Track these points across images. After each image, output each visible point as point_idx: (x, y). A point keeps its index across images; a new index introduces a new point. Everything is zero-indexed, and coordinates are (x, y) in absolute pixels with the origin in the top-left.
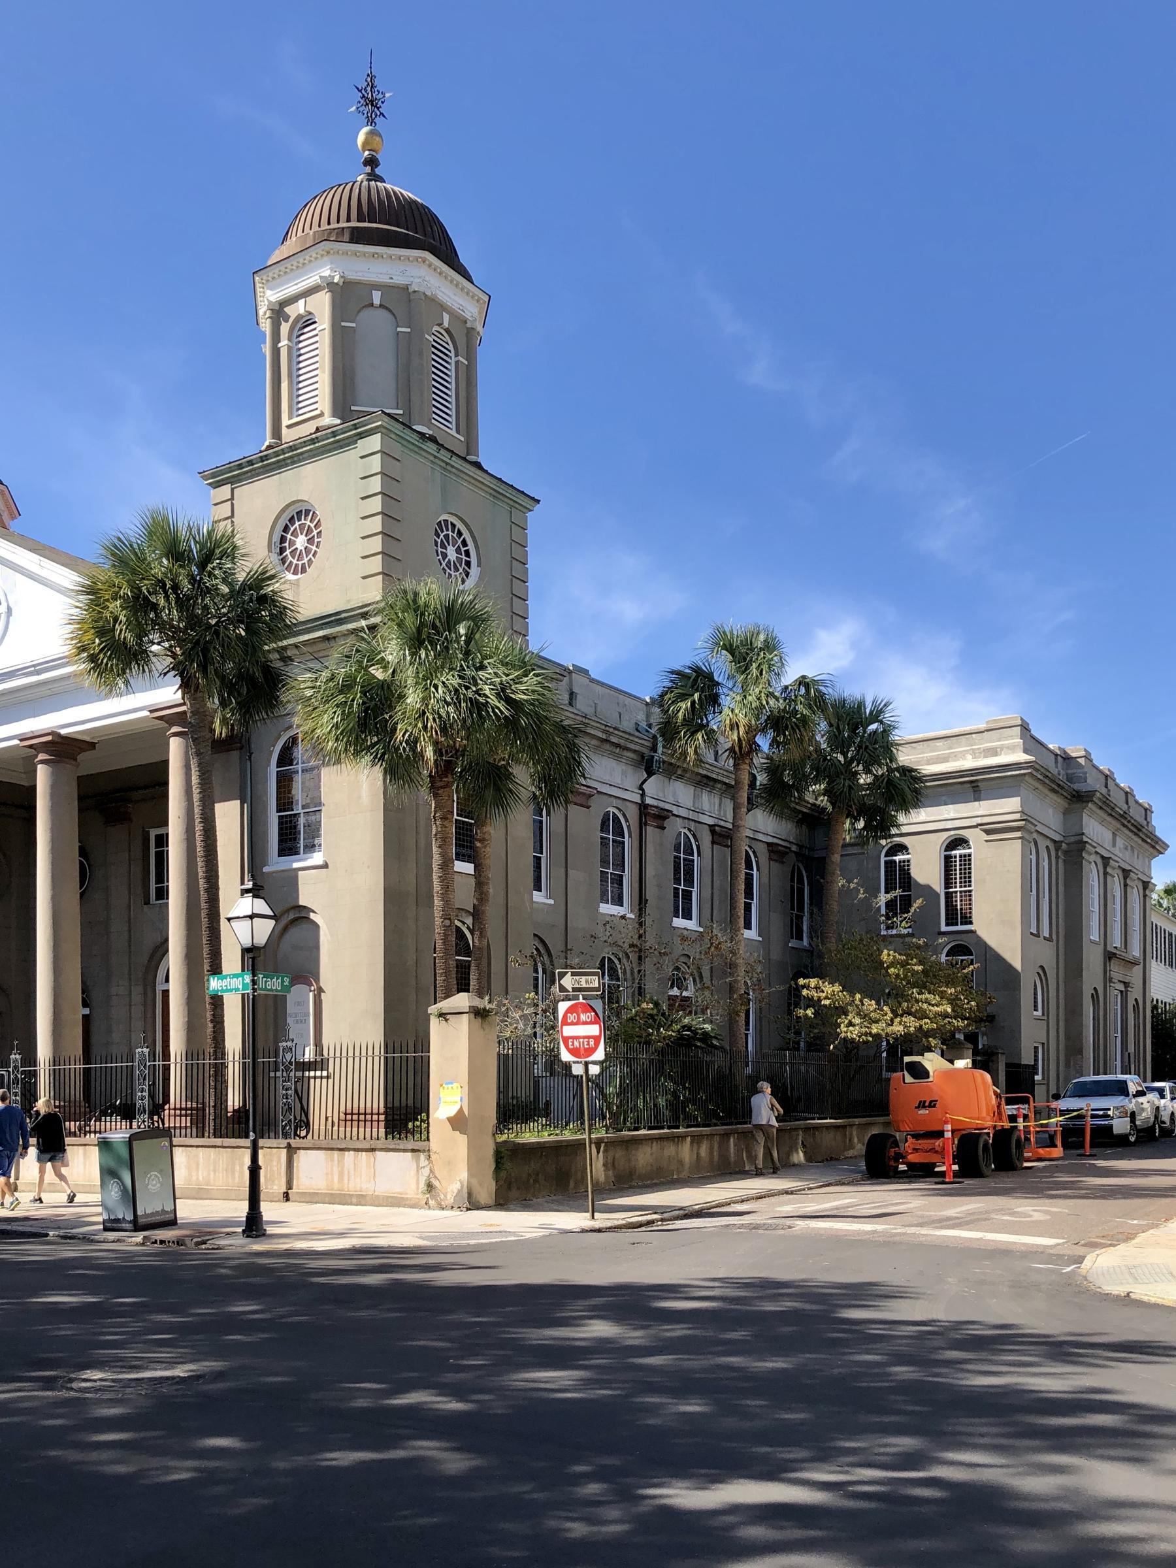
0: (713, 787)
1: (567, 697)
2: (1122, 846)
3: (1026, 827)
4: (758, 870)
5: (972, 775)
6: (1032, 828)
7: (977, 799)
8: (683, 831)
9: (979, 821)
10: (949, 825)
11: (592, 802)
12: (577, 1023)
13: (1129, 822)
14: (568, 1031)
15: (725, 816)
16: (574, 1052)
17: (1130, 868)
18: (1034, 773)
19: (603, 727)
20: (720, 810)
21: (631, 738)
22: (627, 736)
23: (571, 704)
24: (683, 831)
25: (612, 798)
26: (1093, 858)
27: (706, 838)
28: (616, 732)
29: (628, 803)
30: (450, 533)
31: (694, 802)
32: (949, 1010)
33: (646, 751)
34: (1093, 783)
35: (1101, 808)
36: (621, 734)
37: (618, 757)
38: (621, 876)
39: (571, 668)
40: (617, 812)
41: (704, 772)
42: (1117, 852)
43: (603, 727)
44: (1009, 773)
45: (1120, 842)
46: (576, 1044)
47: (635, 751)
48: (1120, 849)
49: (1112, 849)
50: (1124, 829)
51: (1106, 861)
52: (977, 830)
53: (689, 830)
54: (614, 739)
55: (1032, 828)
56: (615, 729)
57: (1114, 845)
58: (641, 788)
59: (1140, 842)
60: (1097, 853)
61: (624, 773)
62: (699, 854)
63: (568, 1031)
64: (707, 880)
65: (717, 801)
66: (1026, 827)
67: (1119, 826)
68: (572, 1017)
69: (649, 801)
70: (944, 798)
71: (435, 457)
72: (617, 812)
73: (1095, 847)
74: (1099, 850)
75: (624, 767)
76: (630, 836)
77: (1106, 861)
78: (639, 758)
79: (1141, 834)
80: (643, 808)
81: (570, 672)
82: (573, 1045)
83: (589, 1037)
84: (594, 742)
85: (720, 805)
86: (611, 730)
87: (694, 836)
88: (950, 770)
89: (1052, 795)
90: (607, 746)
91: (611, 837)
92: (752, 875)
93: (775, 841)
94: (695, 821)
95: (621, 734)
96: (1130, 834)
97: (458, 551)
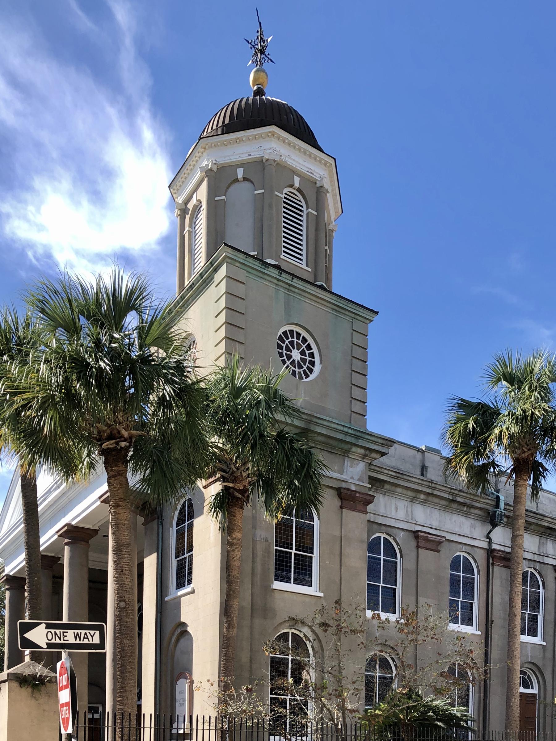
19: (449, 490)
22: (472, 497)
28: (462, 494)
31: (539, 548)
33: (490, 508)
40: (466, 555)
43: (449, 490)
47: (481, 509)
54: (459, 499)
56: (460, 491)
61: (472, 526)
72: (466, 555)
75: (472, 521)
78: (486, 514)
84: (444, 502)
86: (456, 492)
90: (455, 506)
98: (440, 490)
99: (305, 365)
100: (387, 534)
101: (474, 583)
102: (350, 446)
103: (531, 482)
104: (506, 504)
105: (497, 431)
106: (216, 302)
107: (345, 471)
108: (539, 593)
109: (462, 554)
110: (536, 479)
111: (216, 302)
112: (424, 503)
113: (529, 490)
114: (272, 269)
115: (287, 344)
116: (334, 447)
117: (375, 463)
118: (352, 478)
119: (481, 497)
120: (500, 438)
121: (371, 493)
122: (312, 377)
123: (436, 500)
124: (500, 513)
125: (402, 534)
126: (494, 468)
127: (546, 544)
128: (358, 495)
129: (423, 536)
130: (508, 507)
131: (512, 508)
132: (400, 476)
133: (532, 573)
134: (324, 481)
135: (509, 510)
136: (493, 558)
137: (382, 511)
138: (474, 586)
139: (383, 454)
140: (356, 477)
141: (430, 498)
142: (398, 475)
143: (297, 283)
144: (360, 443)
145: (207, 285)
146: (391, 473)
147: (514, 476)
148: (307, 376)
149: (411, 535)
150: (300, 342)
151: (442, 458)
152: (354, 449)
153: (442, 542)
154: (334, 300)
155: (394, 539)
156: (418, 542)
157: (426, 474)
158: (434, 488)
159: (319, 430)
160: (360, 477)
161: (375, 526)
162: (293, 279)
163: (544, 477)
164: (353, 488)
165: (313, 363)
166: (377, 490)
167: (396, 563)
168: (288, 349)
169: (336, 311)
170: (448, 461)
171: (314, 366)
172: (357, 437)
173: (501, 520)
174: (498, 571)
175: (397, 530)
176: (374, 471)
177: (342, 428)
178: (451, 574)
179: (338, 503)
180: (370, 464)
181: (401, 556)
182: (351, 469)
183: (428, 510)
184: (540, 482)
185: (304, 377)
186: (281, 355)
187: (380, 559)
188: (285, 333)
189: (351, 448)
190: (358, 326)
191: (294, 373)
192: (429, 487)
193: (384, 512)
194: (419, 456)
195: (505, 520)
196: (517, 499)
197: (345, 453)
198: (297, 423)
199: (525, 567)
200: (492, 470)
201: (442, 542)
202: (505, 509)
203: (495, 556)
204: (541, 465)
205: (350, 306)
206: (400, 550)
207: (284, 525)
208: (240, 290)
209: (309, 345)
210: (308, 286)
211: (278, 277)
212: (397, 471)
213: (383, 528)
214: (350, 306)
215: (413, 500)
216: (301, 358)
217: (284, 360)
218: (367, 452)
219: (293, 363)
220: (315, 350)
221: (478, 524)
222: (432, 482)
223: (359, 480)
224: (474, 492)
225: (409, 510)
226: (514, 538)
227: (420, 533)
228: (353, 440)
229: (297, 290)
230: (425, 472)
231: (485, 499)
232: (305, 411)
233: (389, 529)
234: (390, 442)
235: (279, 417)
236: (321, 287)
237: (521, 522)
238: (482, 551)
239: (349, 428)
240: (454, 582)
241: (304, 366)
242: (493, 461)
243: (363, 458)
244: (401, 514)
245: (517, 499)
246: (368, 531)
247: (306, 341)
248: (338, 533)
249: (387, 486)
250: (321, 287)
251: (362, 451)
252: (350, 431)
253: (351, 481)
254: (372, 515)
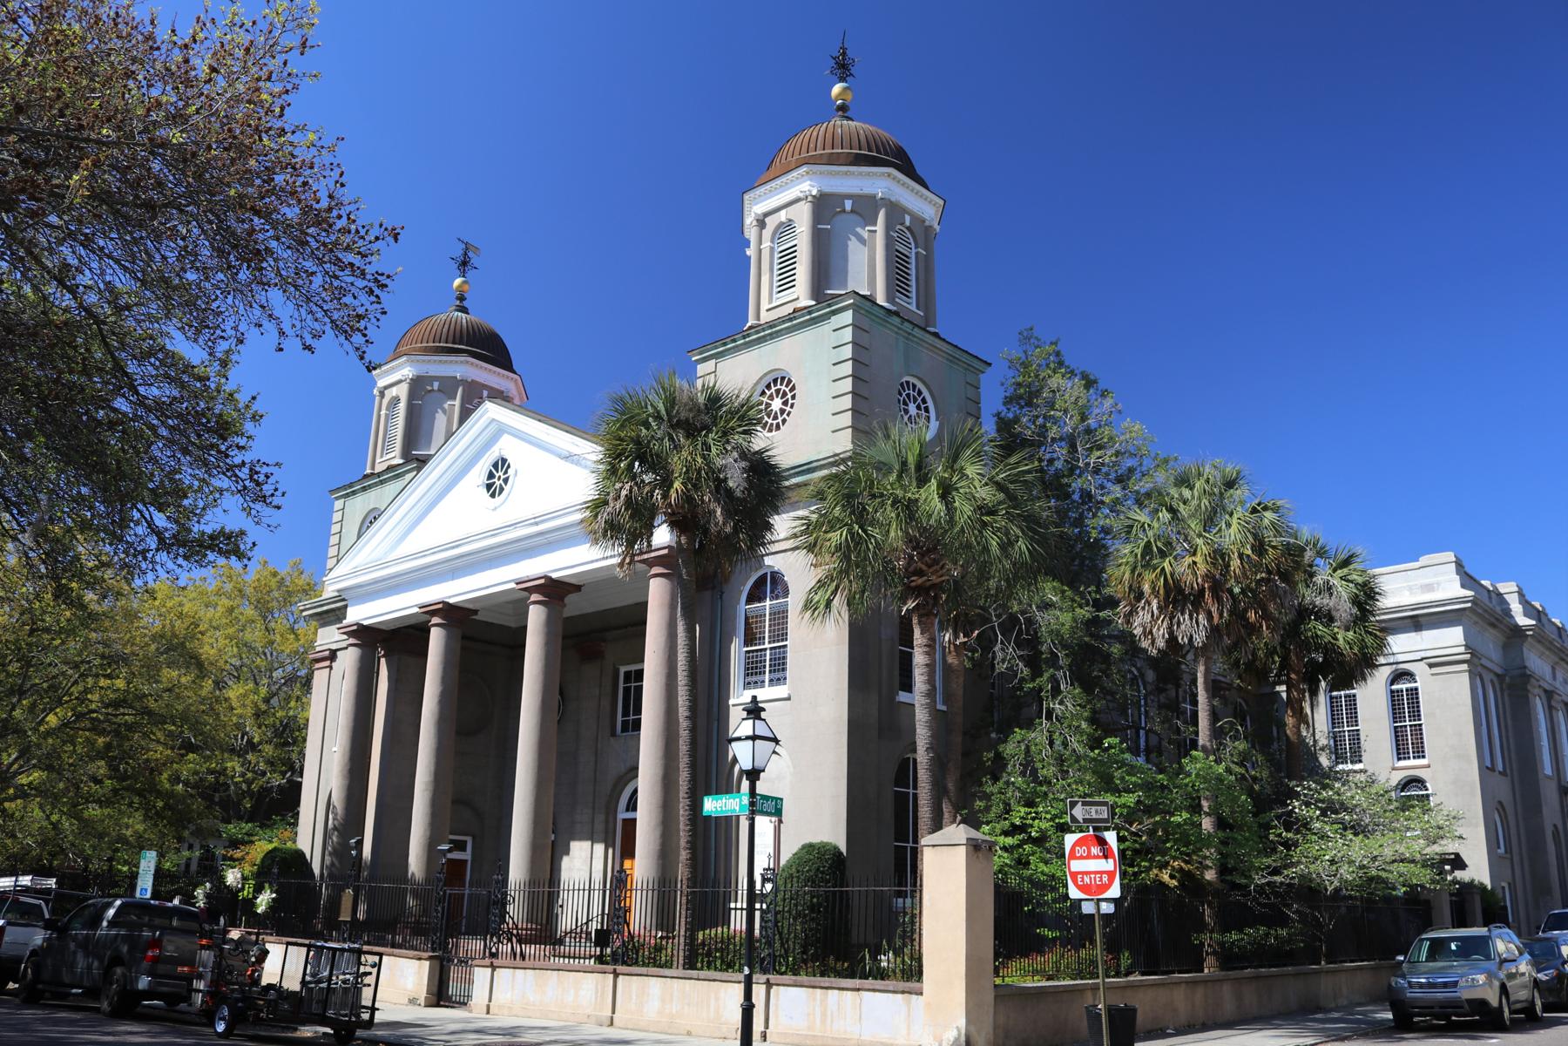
12: (1089, 857)
14: (1076, 866)
16: (1082, 888)
26: (1537, 691)
30: (911, 392)
42: (1558, 684)
46: (1087, 880)
50: (1562, 663)
55: (1475, 660)
57: (1554, 678)
60: (1540, 686)
63: (1076, 866)
68: (1080, 851)
71: (899, 328)
73: (1538, 681)
74: (1542, 683)
77: (1549, 694)
82: (1083, 881)
83: (1102, 873)
89: (1492, 630)
97: (918, 408)
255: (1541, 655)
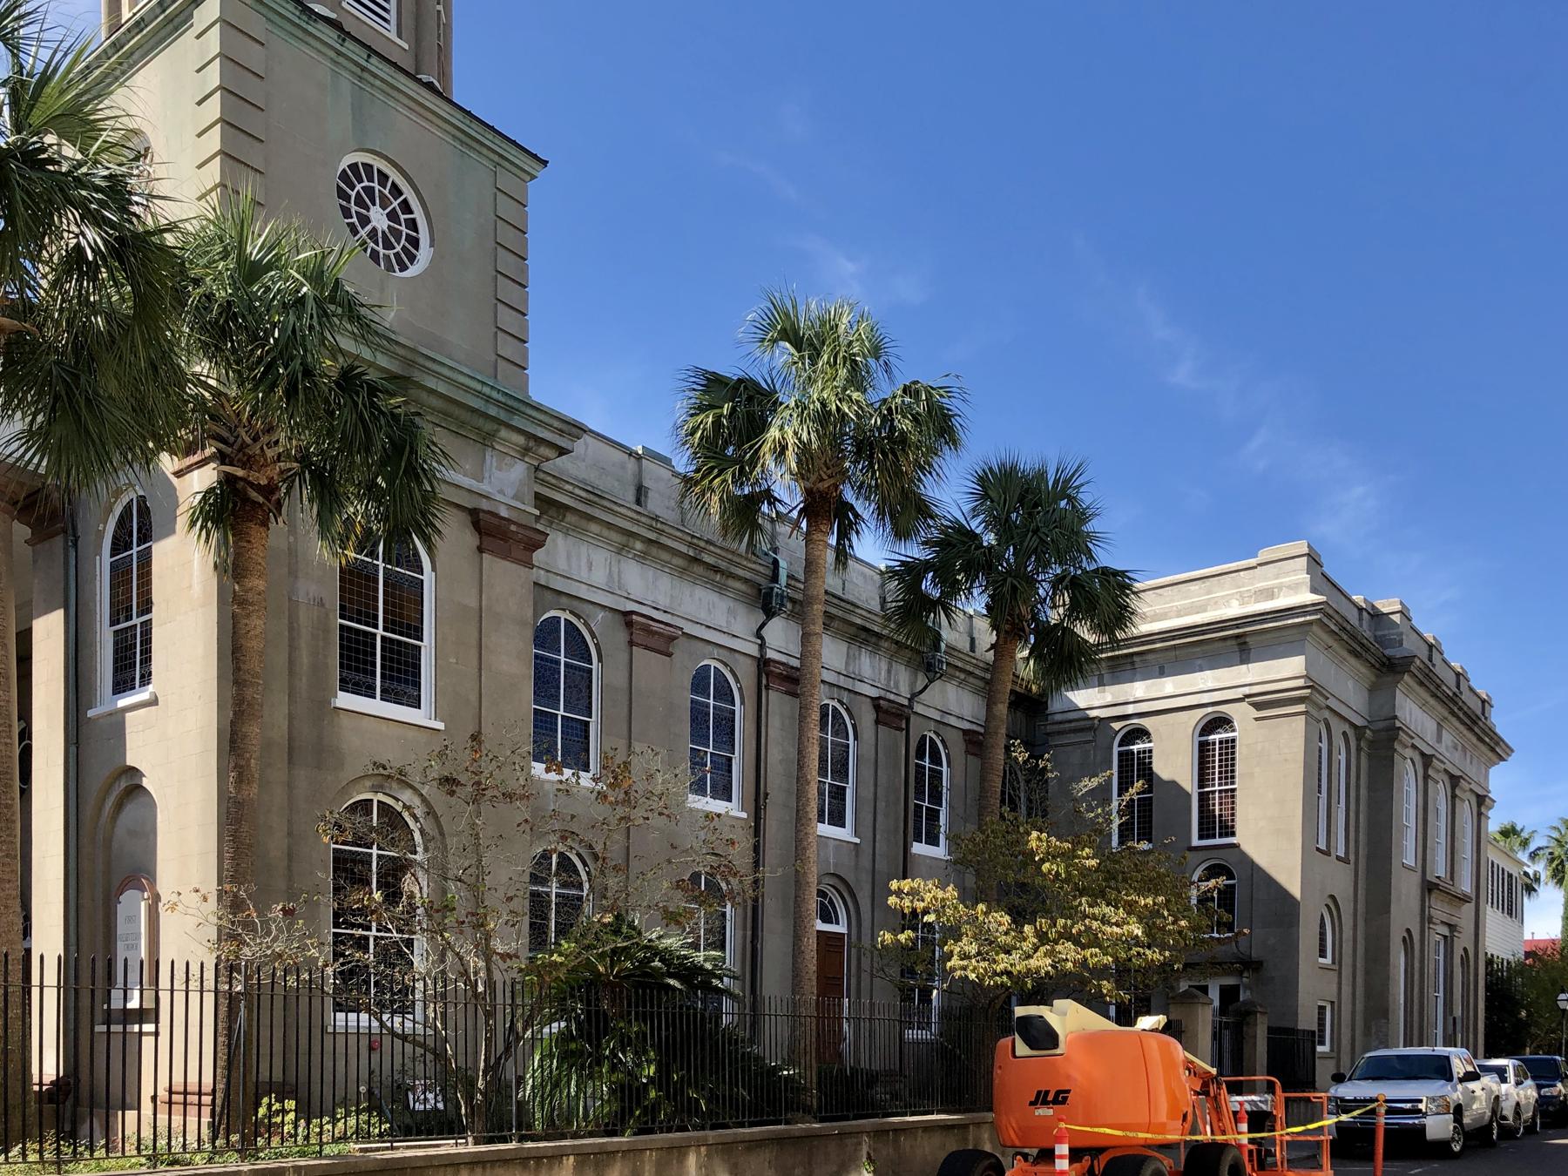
0: (877, 647)
1: (629, 496)
2: (1450, 744)
3: (1312, 696)
4: (949, 765)
5: (1237, 626)
6: (1320, 700)
7: (1245, 660)
8: (832, 703)
9: (1247, 690)
10: (1206, 699)
11: (679, 648)
13: (1460, 709)
15: (897, 687)
17: (1459, 773)
18: (1325, 620)
19: (689, 539)
20: (889, 680)
21: (735, 559)
22: (730, 557)
23: (638, 502)
24: (832, 703)
25: (710, 648)
26: (1409, 753)
27: (867, 717)
28: (712, 548)
29: (737, 655)
31: (847, 664)
32: (1138, 932)
33: (763, 582)
34: (1410, 645)
35: (1421, 684)
36: (718, 551)
37: (721, 589)
38: (730, 759)
39: (640, 452)
41: (859, 621)
42: (1442, 749)
43: (689, 539)
44: (1290, 622)
45: (1447, 737)
47: (746, 581)
48: (1449, 746)
49: (1436, 746)
50: (1453, 720)
51: (1427, 760)
52: (1244, 705)
53: (839, 701)
55: (1320, 700)
56: (708, 542)
57: (1439, 739)
58: (759, 635)
59: (1474, 740)
60: (1414, 747)
62: (856, 738)
64: (868, 774)
65: (884, 666)
66: (1312, 696)
67: (1446, 714)
69: (771, 654)
70: (1199, 662)
73: (1412, 738)
74: (1417, 742)
75: (731, 604)
76: (742, 703)
77: (1427, 760)
78: (754, 592)
79: (1476, 729)
80: (763, 664)
81: (639, 458)
85: (889, 671)
86: (702, 544)
87: (847, 710)
88: (1206, 621)
89: (1352, 660)
91: (711, 701)
92: (940, 773)
93: (974, 727)
94: (849, 690)
95: (718, 551)
96: (1462, 728)
98: (670, 536)
99: (399, 244)
100: (571, 612)
101: (733, 721)
102: (496, 427)
103: (833, 541)
104: (790, 577)
105: (774, 433)
106: (198, 71)
107: (487, 475)
108: (848, 746)
109: (713, 663)
110: (843, 535)
111: (198, 71)
112: (642, 558)
113: (830, 556)
114: (321, 25)
115: (358, 191)
116: (463, 424)
117: (546, 466)
118: (501, 492)
119: (746, 559)
120: (780, 451)
121: (539, 527)
122: (413, 271)
123: (665, 556)
124: (780, 592)
125: (601, 615)
126: (770, 504)
127: (860, 659)
128: (513, 528)
129: (643, 624)
130: (793, 583)
131: (802, 587)
132: (596, 499)
133: (835, 709)
134: (444, 492)
135: (795, 588)
136: (767, 675)
137: (561, 565)
138: (734, 726)
139: (562, 452)
140: (510, 492)
141: (654, 551)
142: (592, 497)
143: (375, 65)
144: (517, 421)
145: (176, 29)
146: (577, 491)
147: (804, 525)
148: (403, 268)
149: (618, 617)
150: (386, 192)
151: (676, 474)
152: (504, 433)
153: (676, 638)
154: (457, 118)
155: (586, 624)
156: (632, 634)
157: (646, 502)
158: (660, 532)
159: (431, 383)
160: (518, 491)
161: (548, 596)
162: (369, 56)
163: (857, 533)
164: (504, 513)
165: (415, 242)
166: (552, 523)
167: (590, 671)
168: (360, 202)
169: (462, 142)
170: (688, 481)
171: (417, 248)
172: (511, 410)
173: (782, 605)
174: (776, 700)
175: (591, 607)
176: (543, 483)
177: (478, 387)
178: (693, 701)
179: (470, 539)
180: (537, 469)
181: (600, 660)
182: (497, 474)
183: (650, 573)
184: (849, 540)
185: (397, 268)
186: (346, 213)
187: (558, 662)
188: (354, 167)
189: (498, 431)
190: (506, 181)
191: (375, 256)
192: (651, 528)
193: (566, 568)
194: (631, 464)
195: (789, 606)
196: (811, 565)
197: (486, 440)
198: (382, 361)
199: (822, 697)
200: (765, 508)
201: (676, 638)
202: (788, 586)
203: (772, 672)
204: (852, 508)
205: (488, 139)
206: (597, 646)
207: (359, 576)
208: (253, 56)
209: (405, 202)
210: (402, 78)
211: (338, 46)
212: (589, 488)
213: (564, 600)
214: (488, 139)
215: (621, 550)
216: (389, 227)
217: (353, 224)
218: (531, 444)
219: (373, 234)
220: (418, 214)
221: (741, 609)
222: (656, 519)
223: (515, 497)
224: (735, 546)
225: (615, 570)
226: (806, 638)
227: (634, 617)
228: (503, 415)
229: (378, 83)
230: (643, 498)
231: (755, 563)
232: (401, 340)
233: (576, 603)
234: (576, 429)
235: (346, 344)
236: (429, 86)
237: (818, 609)
238: (749, 661)
239: (492, 387)
240: (698, 715)
241: (396, 244)
242: (768, 490)
243: (524, 455)
244: (599, 577)
245: (811, 565)
246: (535, 604)
247: (400, 193)
248: (474, 604)
249: (570, 518)
250: (429, 86)
251: (521, 440)
252: (494, 394)
253: (499, 497)
254: (542, 572)
255: (1423, 705)
